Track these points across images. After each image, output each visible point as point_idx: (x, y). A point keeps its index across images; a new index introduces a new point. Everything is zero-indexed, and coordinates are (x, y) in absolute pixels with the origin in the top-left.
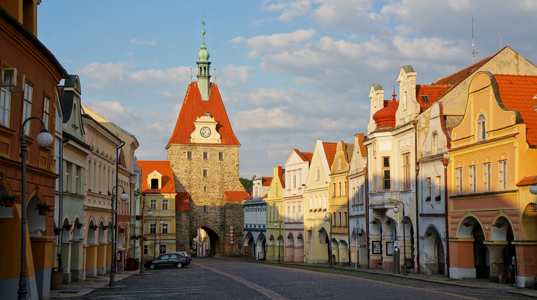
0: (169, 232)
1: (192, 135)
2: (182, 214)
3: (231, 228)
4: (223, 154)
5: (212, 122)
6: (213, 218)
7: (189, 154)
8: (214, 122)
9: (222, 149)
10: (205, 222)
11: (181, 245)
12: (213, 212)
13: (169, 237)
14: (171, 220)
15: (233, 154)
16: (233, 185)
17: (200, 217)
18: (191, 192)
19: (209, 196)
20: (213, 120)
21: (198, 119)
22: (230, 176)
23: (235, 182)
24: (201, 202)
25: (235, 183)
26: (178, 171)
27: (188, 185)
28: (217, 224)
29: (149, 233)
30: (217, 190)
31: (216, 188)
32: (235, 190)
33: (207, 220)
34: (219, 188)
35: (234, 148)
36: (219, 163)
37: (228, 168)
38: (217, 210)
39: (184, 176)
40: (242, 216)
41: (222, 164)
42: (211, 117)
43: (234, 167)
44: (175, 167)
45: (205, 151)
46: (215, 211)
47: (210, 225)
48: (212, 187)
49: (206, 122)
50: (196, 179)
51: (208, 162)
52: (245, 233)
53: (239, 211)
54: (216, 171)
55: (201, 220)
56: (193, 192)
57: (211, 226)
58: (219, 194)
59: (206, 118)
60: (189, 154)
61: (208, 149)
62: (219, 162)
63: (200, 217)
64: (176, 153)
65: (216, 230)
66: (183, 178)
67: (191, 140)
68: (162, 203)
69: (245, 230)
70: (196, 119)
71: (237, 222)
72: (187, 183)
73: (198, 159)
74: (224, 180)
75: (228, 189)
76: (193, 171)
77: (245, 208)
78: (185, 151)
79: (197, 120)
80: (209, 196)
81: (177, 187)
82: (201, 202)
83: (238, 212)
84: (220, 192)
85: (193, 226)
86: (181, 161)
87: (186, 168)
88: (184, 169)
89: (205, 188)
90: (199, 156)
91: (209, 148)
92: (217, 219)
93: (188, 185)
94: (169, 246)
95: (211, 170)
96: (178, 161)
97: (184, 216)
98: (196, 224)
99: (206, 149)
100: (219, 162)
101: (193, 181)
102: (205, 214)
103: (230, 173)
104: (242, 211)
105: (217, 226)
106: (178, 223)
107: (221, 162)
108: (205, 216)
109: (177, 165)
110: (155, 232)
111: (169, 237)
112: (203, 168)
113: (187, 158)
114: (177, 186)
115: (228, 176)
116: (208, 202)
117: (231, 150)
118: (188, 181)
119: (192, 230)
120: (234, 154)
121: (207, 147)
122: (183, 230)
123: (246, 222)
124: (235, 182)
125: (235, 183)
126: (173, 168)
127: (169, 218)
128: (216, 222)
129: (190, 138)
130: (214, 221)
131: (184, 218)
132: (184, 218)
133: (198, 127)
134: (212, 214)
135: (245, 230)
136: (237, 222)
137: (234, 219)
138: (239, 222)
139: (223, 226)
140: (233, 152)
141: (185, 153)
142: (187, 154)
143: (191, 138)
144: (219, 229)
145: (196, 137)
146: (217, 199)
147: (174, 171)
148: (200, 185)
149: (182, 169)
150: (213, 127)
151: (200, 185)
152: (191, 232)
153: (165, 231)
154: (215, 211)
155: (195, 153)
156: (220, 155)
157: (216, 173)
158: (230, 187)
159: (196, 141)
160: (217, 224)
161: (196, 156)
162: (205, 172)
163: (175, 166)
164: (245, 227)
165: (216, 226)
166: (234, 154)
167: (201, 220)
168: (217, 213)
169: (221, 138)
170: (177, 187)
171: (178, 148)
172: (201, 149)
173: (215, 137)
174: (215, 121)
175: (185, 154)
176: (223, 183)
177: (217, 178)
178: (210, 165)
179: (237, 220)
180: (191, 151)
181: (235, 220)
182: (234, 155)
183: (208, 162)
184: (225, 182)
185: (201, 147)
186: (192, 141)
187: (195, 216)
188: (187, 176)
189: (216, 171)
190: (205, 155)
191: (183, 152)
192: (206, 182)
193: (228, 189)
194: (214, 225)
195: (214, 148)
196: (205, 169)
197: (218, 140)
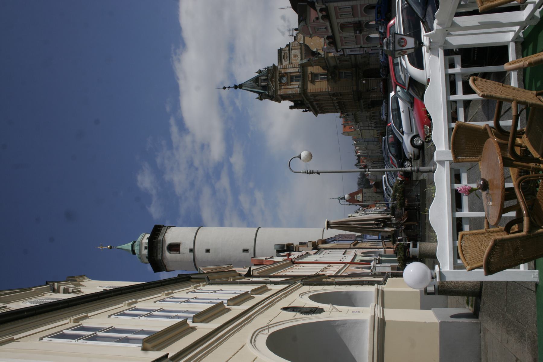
1: (360, 200)
9: (363, 193)
20: (356, 195)
21: (356, 199)
59: (356, 197)
61: (364, 196)
99: (363, 197)
133: (358, 199)
145: (360, 199)
150: (358, 195)
156: (365, 193)
159: (362, 199)
172: (363, 198)
173: (360, 195)
190: (365, 197)
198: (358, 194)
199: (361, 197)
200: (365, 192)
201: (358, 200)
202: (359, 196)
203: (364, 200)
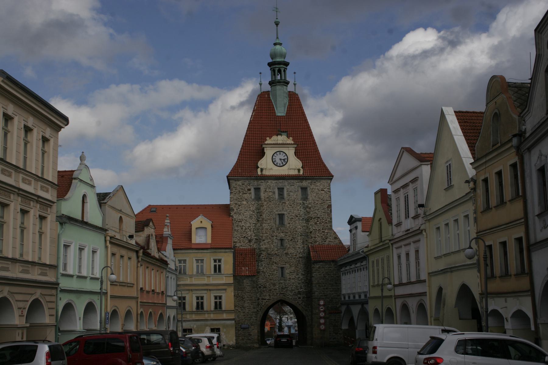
0: (224, 308)
2: (245, 281)
3: (322, 303)
4: (308, 189)
5: (289, 144)
6: (294, 287)
7: (257, 190)
8: (292, 144)
9: (305, 183)
10: (283, 292)
11: (244, 328)
12: (293, 277)
13: (225, 316)
14: (225, 290)
15: (322, 190)
16: (324, 236)
17: (274, 285)
18: (259, 249)
19: (287, 254)
20: (290, 141)
21: (269, 141)
22: (318, 223)
23: (326, 231)
24: (276, 263)
25: (326, 234)
26: (241, 218)
27: (255, 237)
28: (301, 296)
29: (194, 309)
30: (300, 244)
31: (298, 241)
32: (326, 243)
33: (285, 290)
34: (301, 241)
35: (323, 181)
36: (301, 204)
37: (315, 211)
38: (300, 275)
39: (248, 225)
40: (338, 282)
41: (306, 205)
42: (288, 137)
43: (324, 209)
44: (235, 210)
45: (280, 185)
46: (297, 276)
47: (290, 298)
48: (292, 240)
49: (279, 144)
50: (267, 229)
51: (285, 203)
52: (343, 308)
53: (332, 276)
54: (297, 216)
55: (277, 290)
56: (263, 247)
57: (291, 299)
58: (302, 251)
59: (281, 139)
60: (257, 190)
61: (285, 184)
62: (301, 202)
63: (274, 285)
64: (237, 191)
65: (300, 304)
66: (247, 228)
67: (259, 170)
68: (213, 264)
69: (343, 304)
70: (266, 140)
71: (331, 291)
72: (254, 235)
73: (269, 199)
74: (310, 229)
75: (316, 242)
76: (262, 217)
77: (342, 270)
78: (250, 188)
79: (266, 142)
80: (287, 254)
81: (239, 241)
82: (276, 263)
83: (332, 277)
84: (303, 247)
85: (265, 299)
86: (245, 203)
87: (252, 213)
88: (248, 214)
89: (282, 240)
90: (270, 194)
91: (286, 183)
92: (301, 288)
93: (255, 237)
94: (225, 330)
95: (289, 214)
96: (239, 203)
97: (247, 283)
98: (269, 295)
99: (281, 184)
100: (301, 202)
101: (263, 231)
102: (282, 282)
103: (319, 218)
104: (337, 275)
105: (302, 298)
106: (238, 294)
107: (305, 202)
108: (282, 283)
109: (239, 208)
110: (202, 308)
111: (225, 316)
112: (277, 211)
113: (253, 197)
114: (239, 239)
115: (316, 223)
116: (286, 262)
117: (318, 184)
118: (255, 232)
119: (263, 306)
120: (324, 190)
121: (282, 181)
122: (246, 305)
123: (344, 292)
124: (326, 231)
125: (327, 233)
126: (232, 214)
127: (223, 287)
128: (299, 293)
129: (258, 167)
130: (297, 291)
131: (248, 286)
132: (248, 286)
133: (269, 152)
134: (293, 281)
135: (343, 304)
136: (331, 291)
137: (325, 287)
138: (333, 292)
139: (309, 296)
140: (321, 187)
141: (249, 190)
142: (253, 191)
143: (259, 167)
144: (303, 303)
146: (300, 257)
147: (235, 217)
148: (273, 237)
149: (245, 214)
150: (291, 152)
151: (273, 237)
152: (261, 308)
153: (218, 306)
154: (297, 276)
155: (264, 190)
156: (304, 189)
157: (297, 218)
158: (319, 239)
159: (265, 173)
160: (301, 296)
161: (266, 193)
162: (281, 216)
163: (235, 209)
164: (343, 299)
165: (299, 298)
166: (324, 190)
167: (277, 290)
168: (300, 279)
169: (302, 167)
170: (239, 241)
171: (240, 183)
174: (293, 142)
175: (249, 192)
176: (307, 233)
177: (299, 226)
178: (288, 207)
179: (330, 289)
180: (259, 187)
181: (327, 289)
182: (323, 192)
183: (285, 203)
184: (311, 232)
185: (274, 182)
186: (259, 173)
187: (268, 284)
188: (254, 225)
189: (297, 216)
191: (246, 189)
192: (283, 232)
193: (316, 242)
194: (296, 297)
195: (292, 181)
196: (280, 213)
197: (299, 170)
198: (297, 154)
199: (283, 171)
200: (311, 197)
201: (262, 154)
202: (285, 161)
203: (263, 185)
